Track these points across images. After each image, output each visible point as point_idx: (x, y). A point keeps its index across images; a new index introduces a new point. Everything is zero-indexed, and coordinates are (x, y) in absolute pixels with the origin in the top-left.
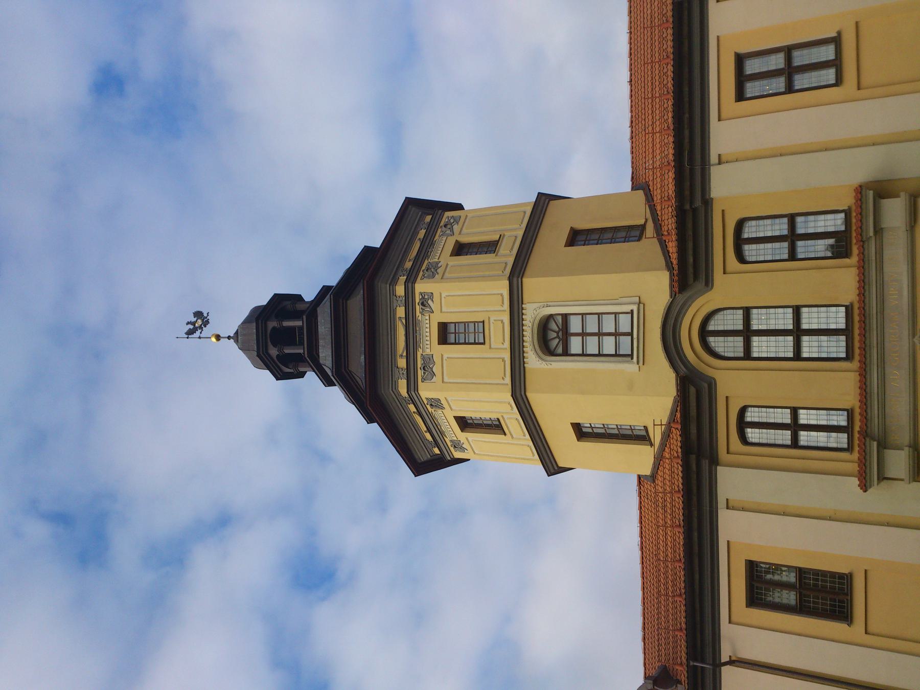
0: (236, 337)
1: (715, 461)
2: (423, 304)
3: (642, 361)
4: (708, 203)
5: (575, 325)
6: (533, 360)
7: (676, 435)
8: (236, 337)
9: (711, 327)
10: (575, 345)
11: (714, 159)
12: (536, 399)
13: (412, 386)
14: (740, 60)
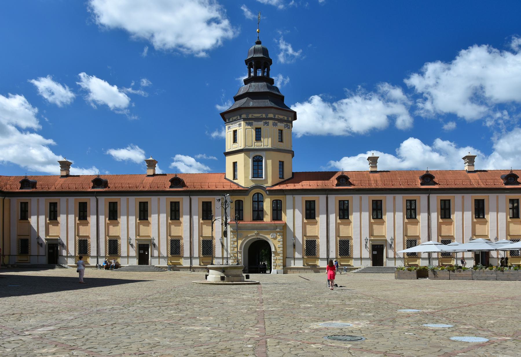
2: (266, 123)
4: (286, 195)
11: (294, 196)
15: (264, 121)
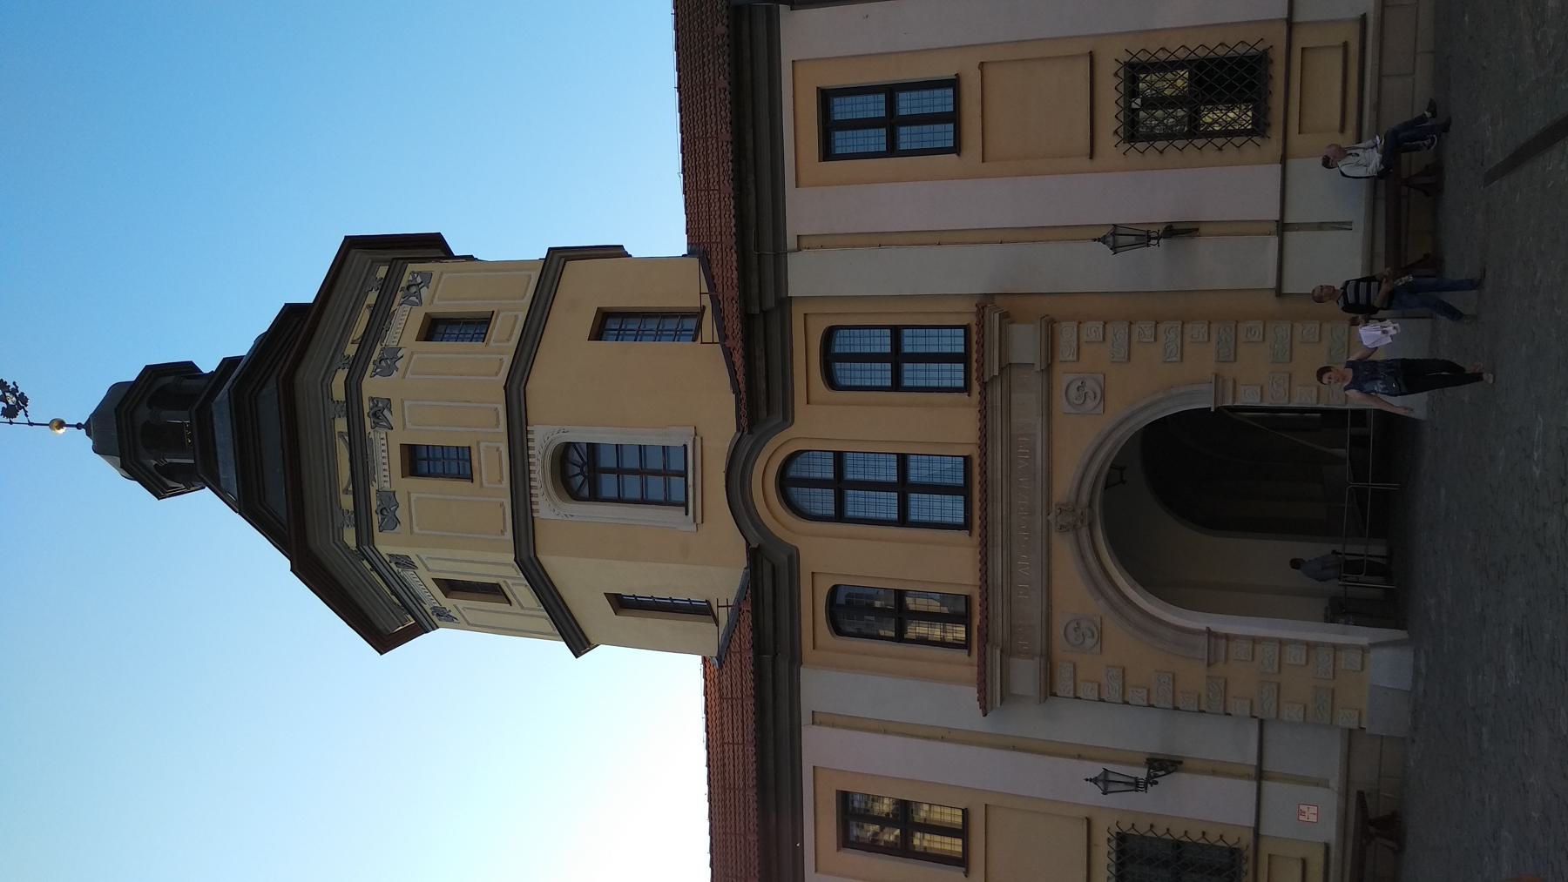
0: (86, 427)
1: (796, 660)
2: (376, 415)
3: (700, 520)
4: (785, 303)
5: (607, 460)
6: (548, 507)
7: (747, 619)
8: (86, 427)
9: (793, 472)
10: (608, 484)
11: (791, 242)
12: (555, 564)
13: (365, 536)
14: (826, 97)
15: (368, 421)
